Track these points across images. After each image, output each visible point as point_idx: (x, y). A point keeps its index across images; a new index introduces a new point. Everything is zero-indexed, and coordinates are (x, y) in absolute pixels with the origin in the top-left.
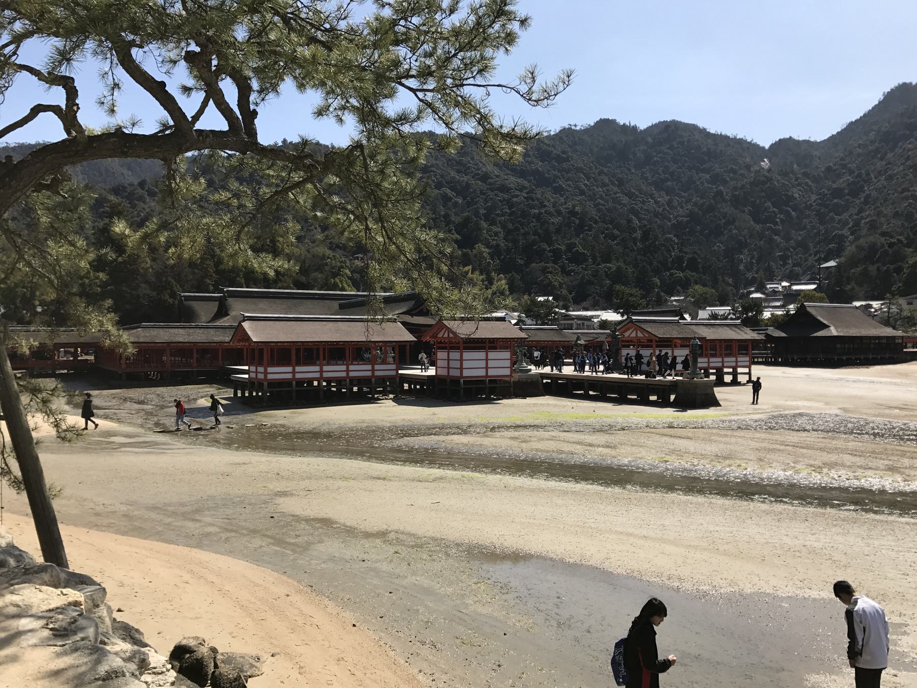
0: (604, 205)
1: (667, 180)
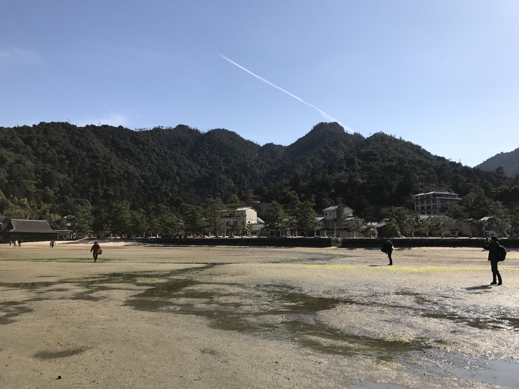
0: (162, 170)
1: (204, 159)
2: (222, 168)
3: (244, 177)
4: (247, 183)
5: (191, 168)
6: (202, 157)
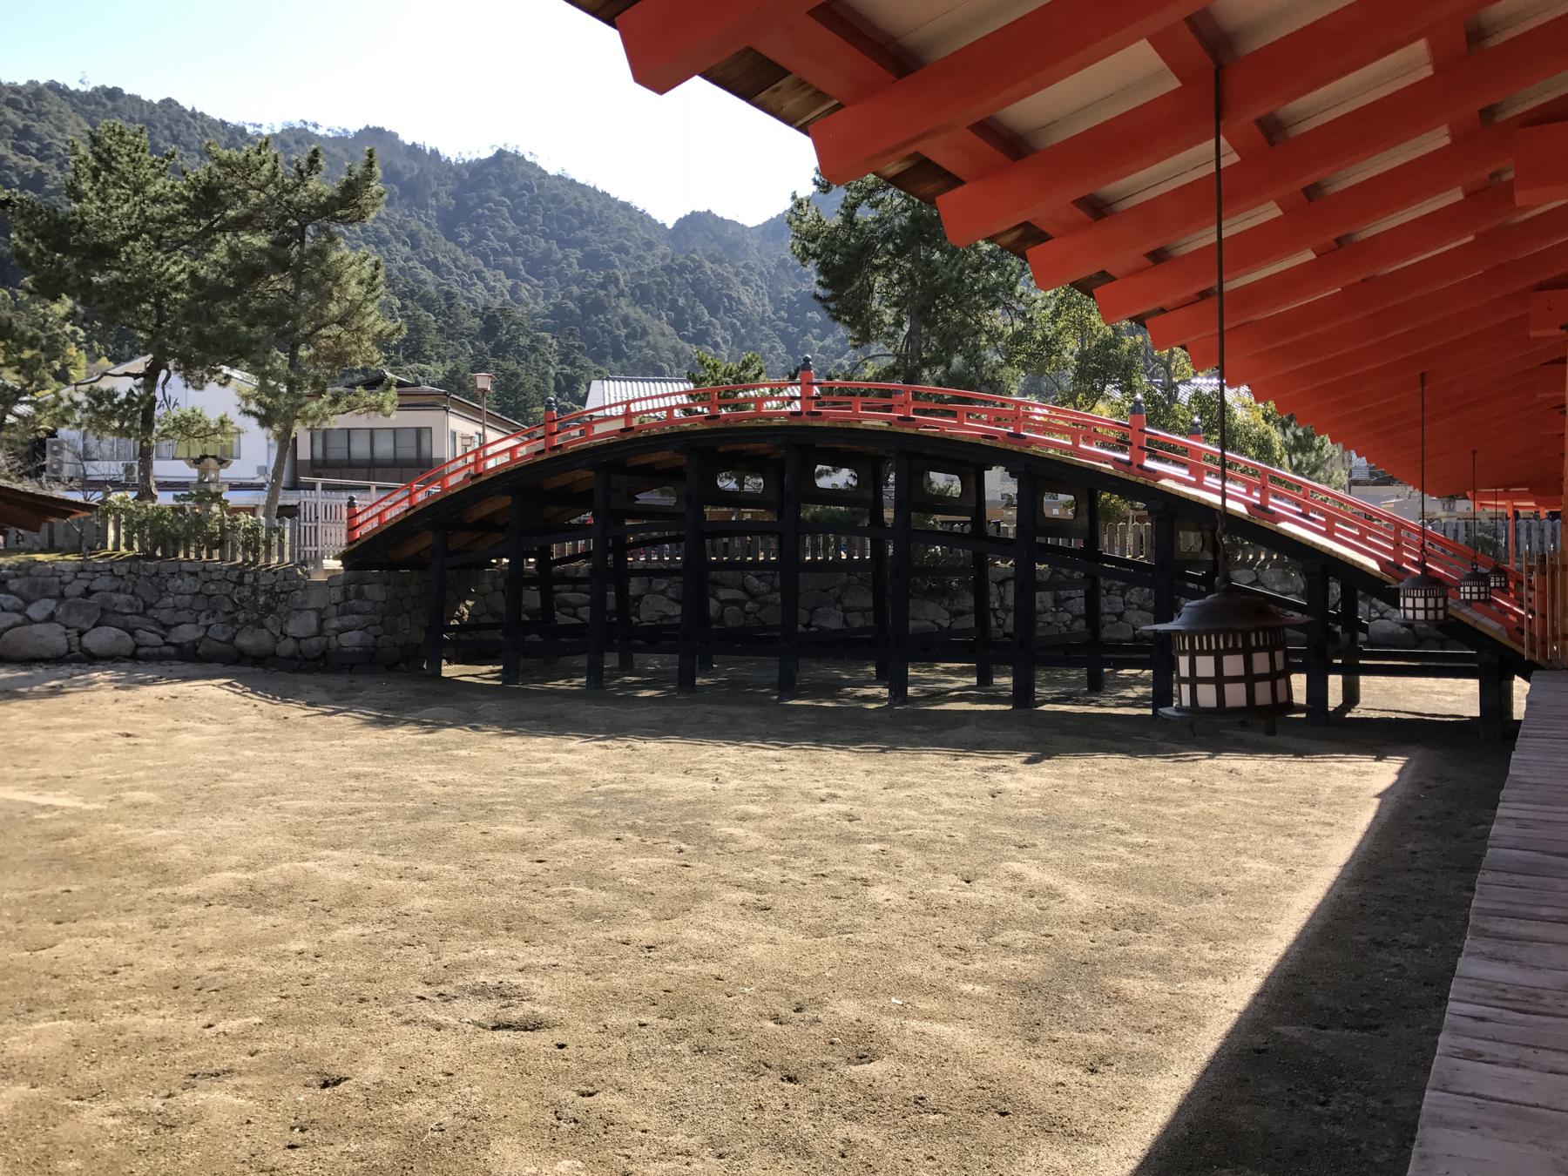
1: (505, 252)
2: (617, 280)
3: (707, 318)
4: (726, 341)
5: (482, 279)
6: (496, 244)
